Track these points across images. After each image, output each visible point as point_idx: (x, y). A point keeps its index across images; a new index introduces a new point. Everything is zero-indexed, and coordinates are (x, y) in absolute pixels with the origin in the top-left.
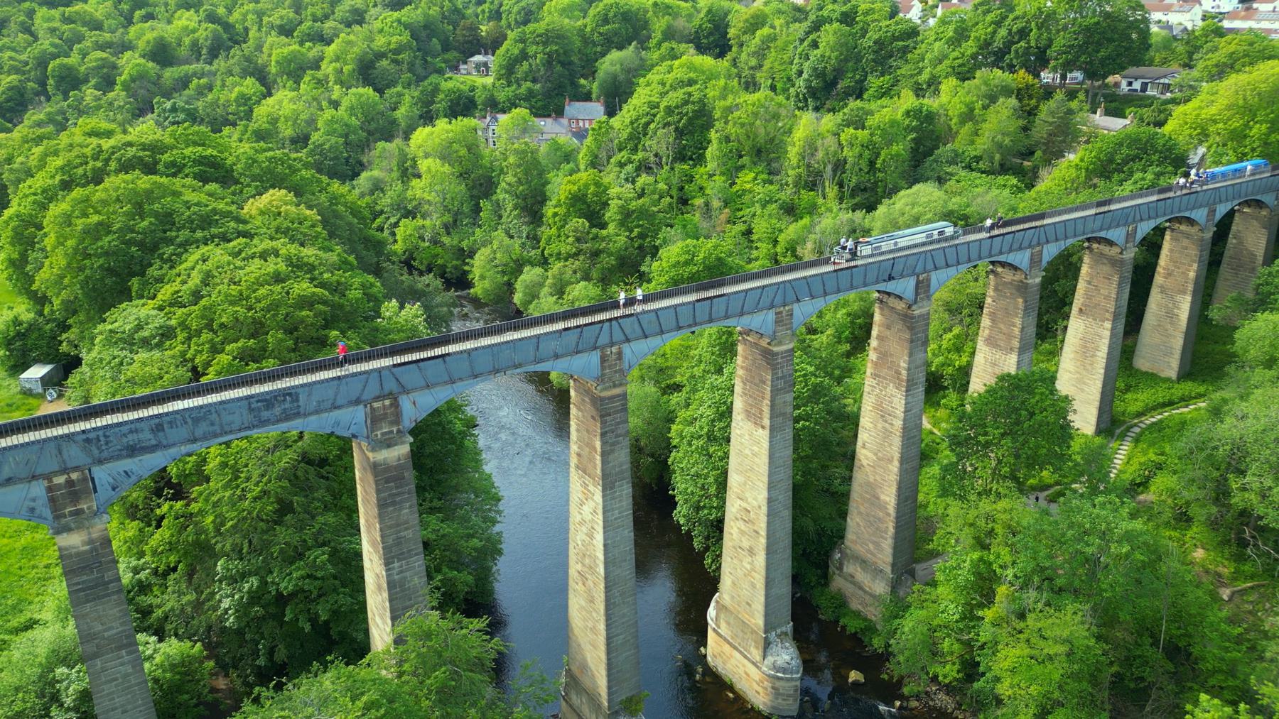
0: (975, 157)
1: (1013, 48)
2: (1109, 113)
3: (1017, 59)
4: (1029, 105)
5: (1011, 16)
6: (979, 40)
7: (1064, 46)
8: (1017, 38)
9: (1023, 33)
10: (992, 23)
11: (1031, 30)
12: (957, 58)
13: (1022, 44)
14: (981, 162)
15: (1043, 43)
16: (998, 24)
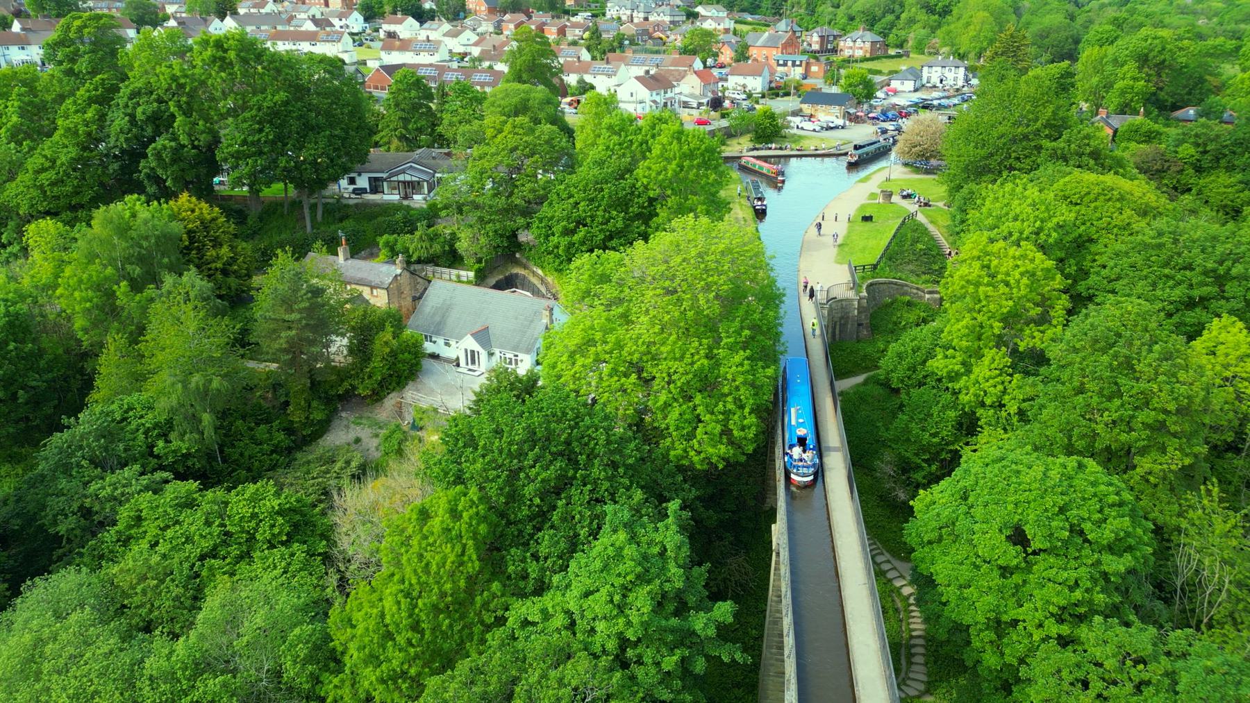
0: (156, 426)
1: (149, 151)
2: (354, 253)
3: (165, 168)
4: (218, 257)
5: (125, 90)
6: (76, 133)
7: (244, 142)
8: (149, 131)
9: (160, 122)
10: (91, 101)
11: (173, 116)
12: (43, 170)
13: (161, 142)
14: (172, 436)
15: (204, 139)
16: (105, 98)
